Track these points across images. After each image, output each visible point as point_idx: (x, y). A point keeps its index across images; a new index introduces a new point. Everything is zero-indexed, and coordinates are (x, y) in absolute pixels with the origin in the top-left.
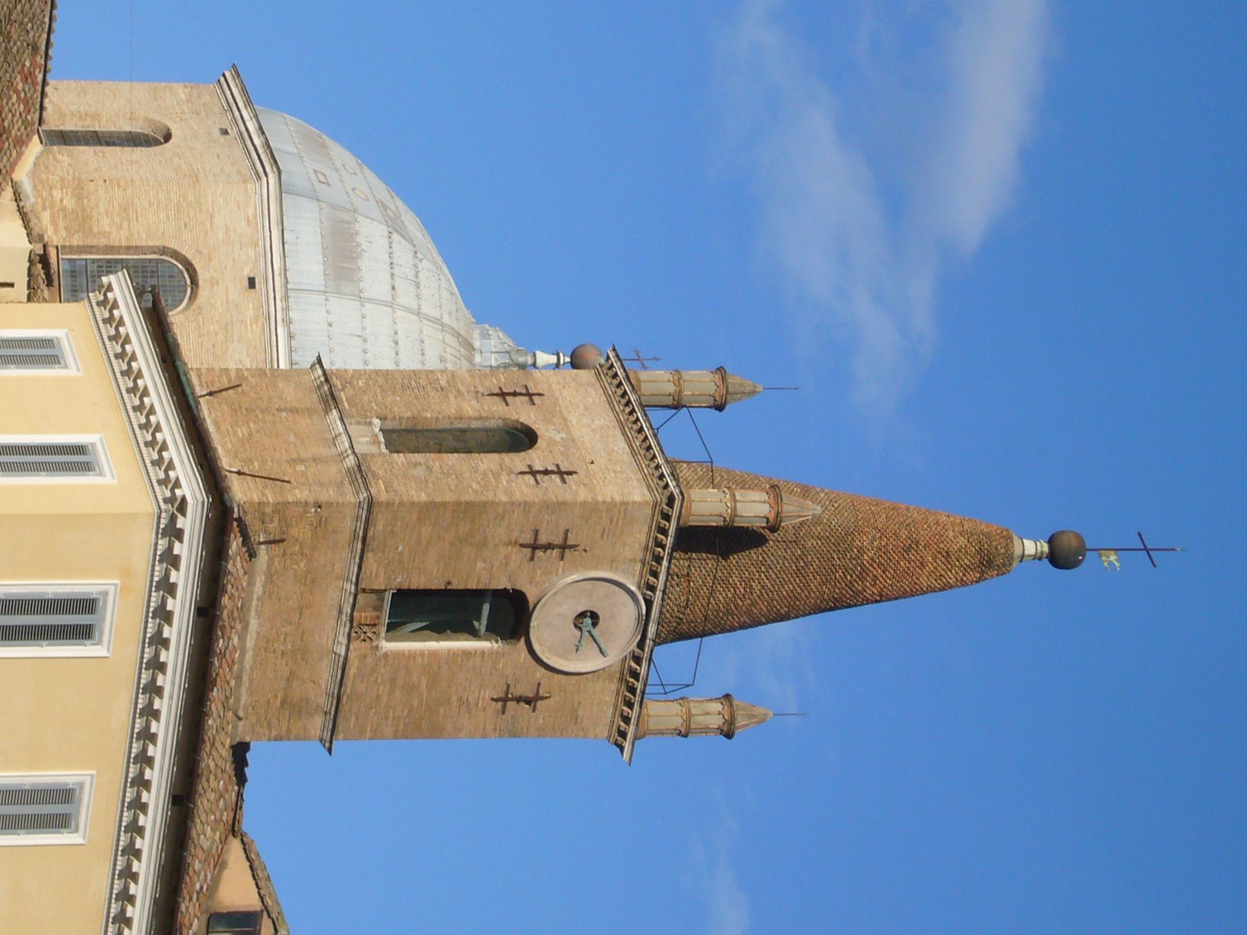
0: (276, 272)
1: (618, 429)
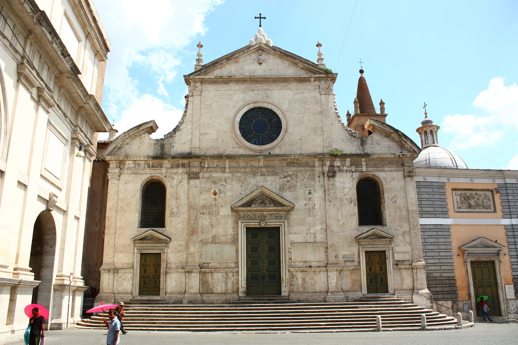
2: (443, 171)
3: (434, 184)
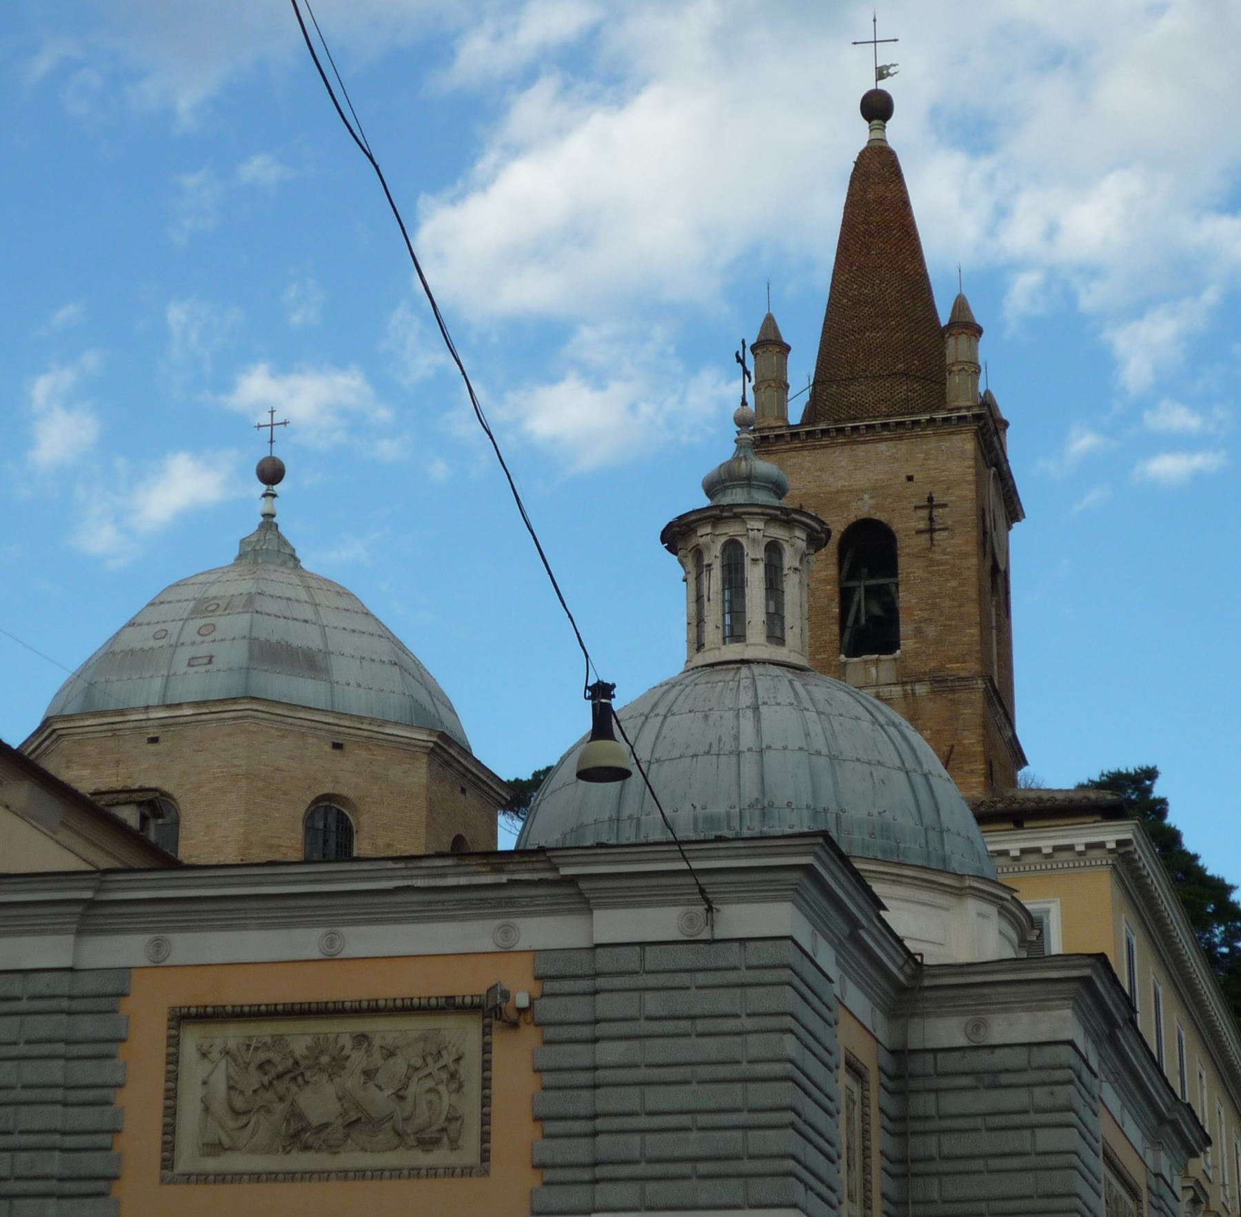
0: (337, 721)
1: (855, 447)
2: (98, 890)
3: (40, 984)
